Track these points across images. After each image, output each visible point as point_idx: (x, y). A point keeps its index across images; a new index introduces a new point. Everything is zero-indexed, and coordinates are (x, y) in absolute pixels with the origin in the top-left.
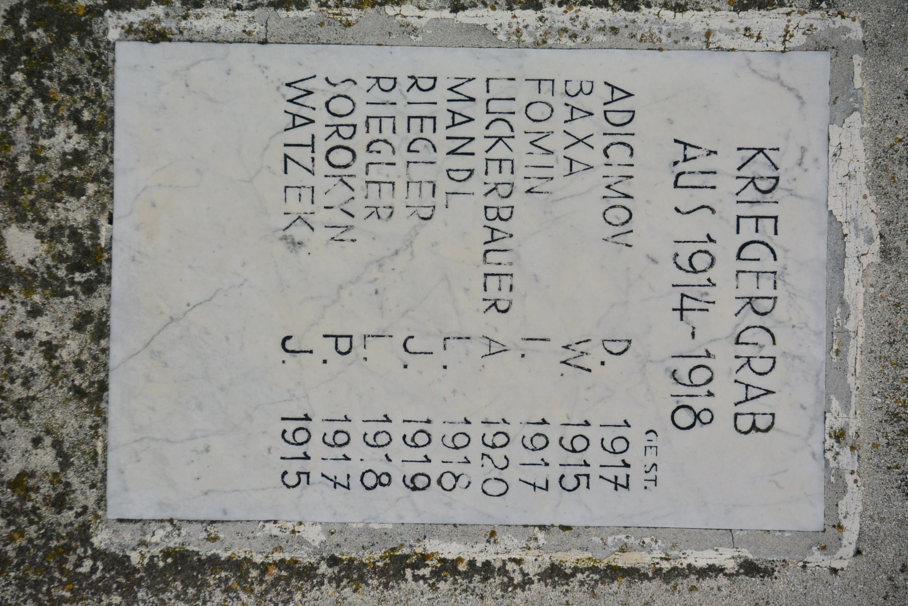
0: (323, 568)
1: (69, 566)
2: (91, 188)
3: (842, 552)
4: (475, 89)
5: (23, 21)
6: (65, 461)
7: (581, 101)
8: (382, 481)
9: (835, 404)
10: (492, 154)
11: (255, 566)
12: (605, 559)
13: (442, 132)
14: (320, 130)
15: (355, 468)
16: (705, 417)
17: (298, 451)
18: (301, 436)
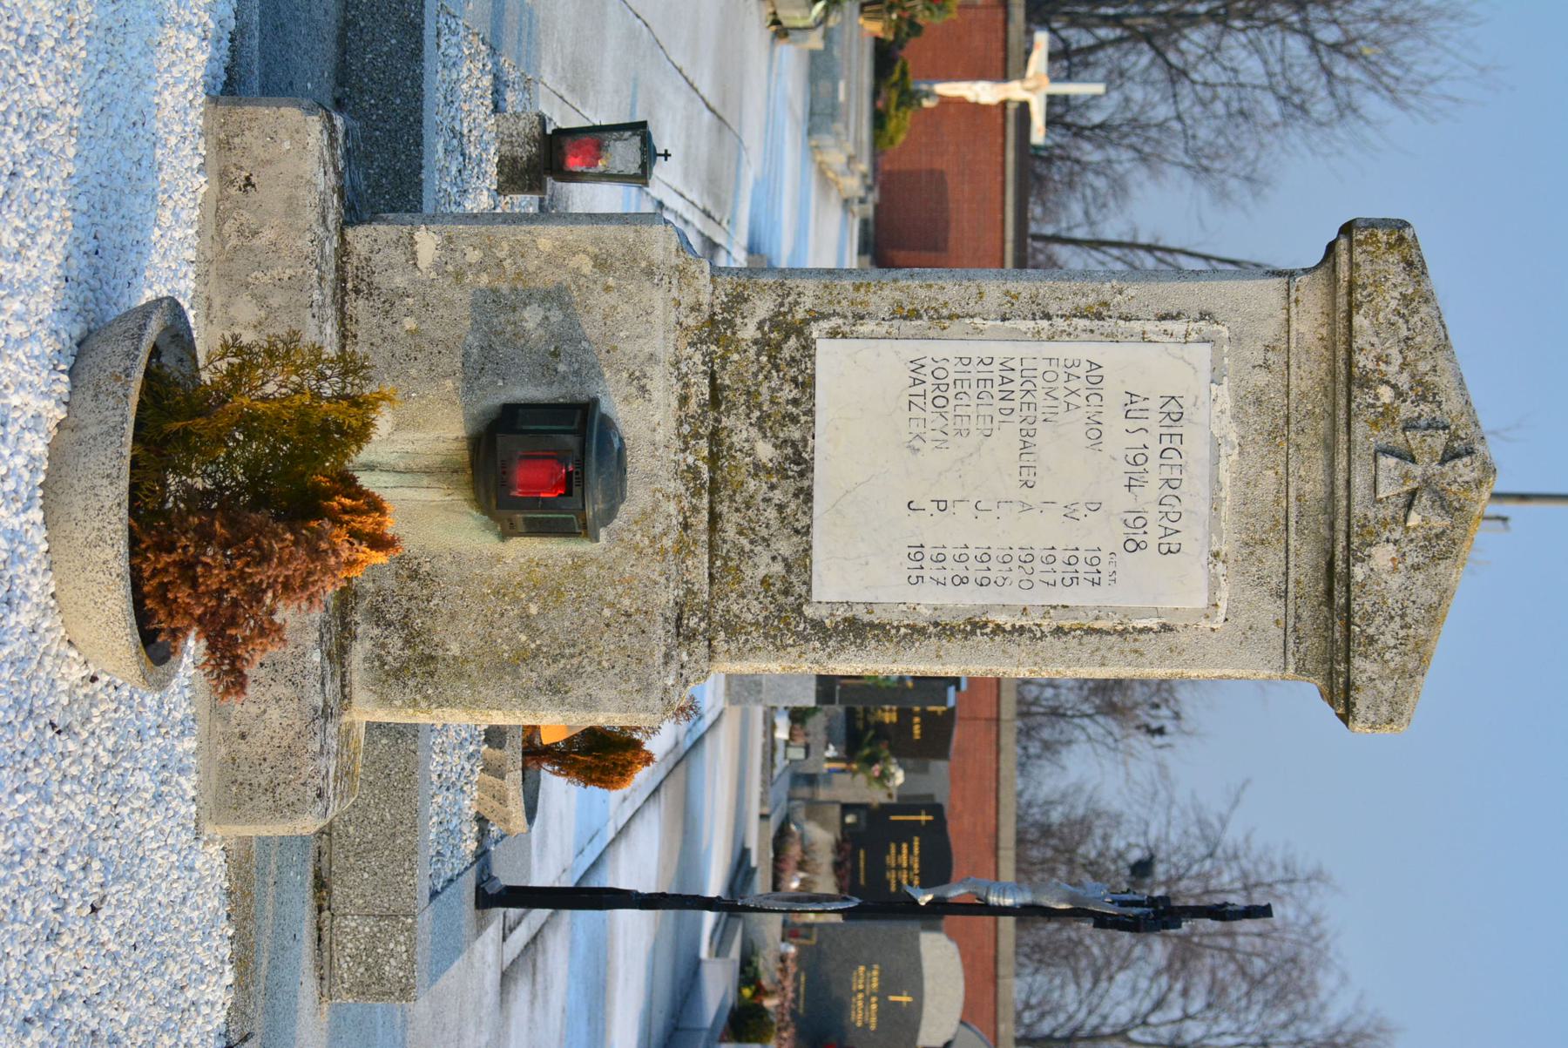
0: (931, 628)
1: (792, 627)
3: (1218, 619)
4: (1015, 364)
5: (766, 329)
6: (789, 568)
8: (964, 581)
9: (1214, 538)
10: (1024, 400)
11: (893, 627)
12: (1088, 623)
13: (997, 388)
14: (929, 387)
16: (1143, 545)
17: (917, 564)
18: (919, 556)
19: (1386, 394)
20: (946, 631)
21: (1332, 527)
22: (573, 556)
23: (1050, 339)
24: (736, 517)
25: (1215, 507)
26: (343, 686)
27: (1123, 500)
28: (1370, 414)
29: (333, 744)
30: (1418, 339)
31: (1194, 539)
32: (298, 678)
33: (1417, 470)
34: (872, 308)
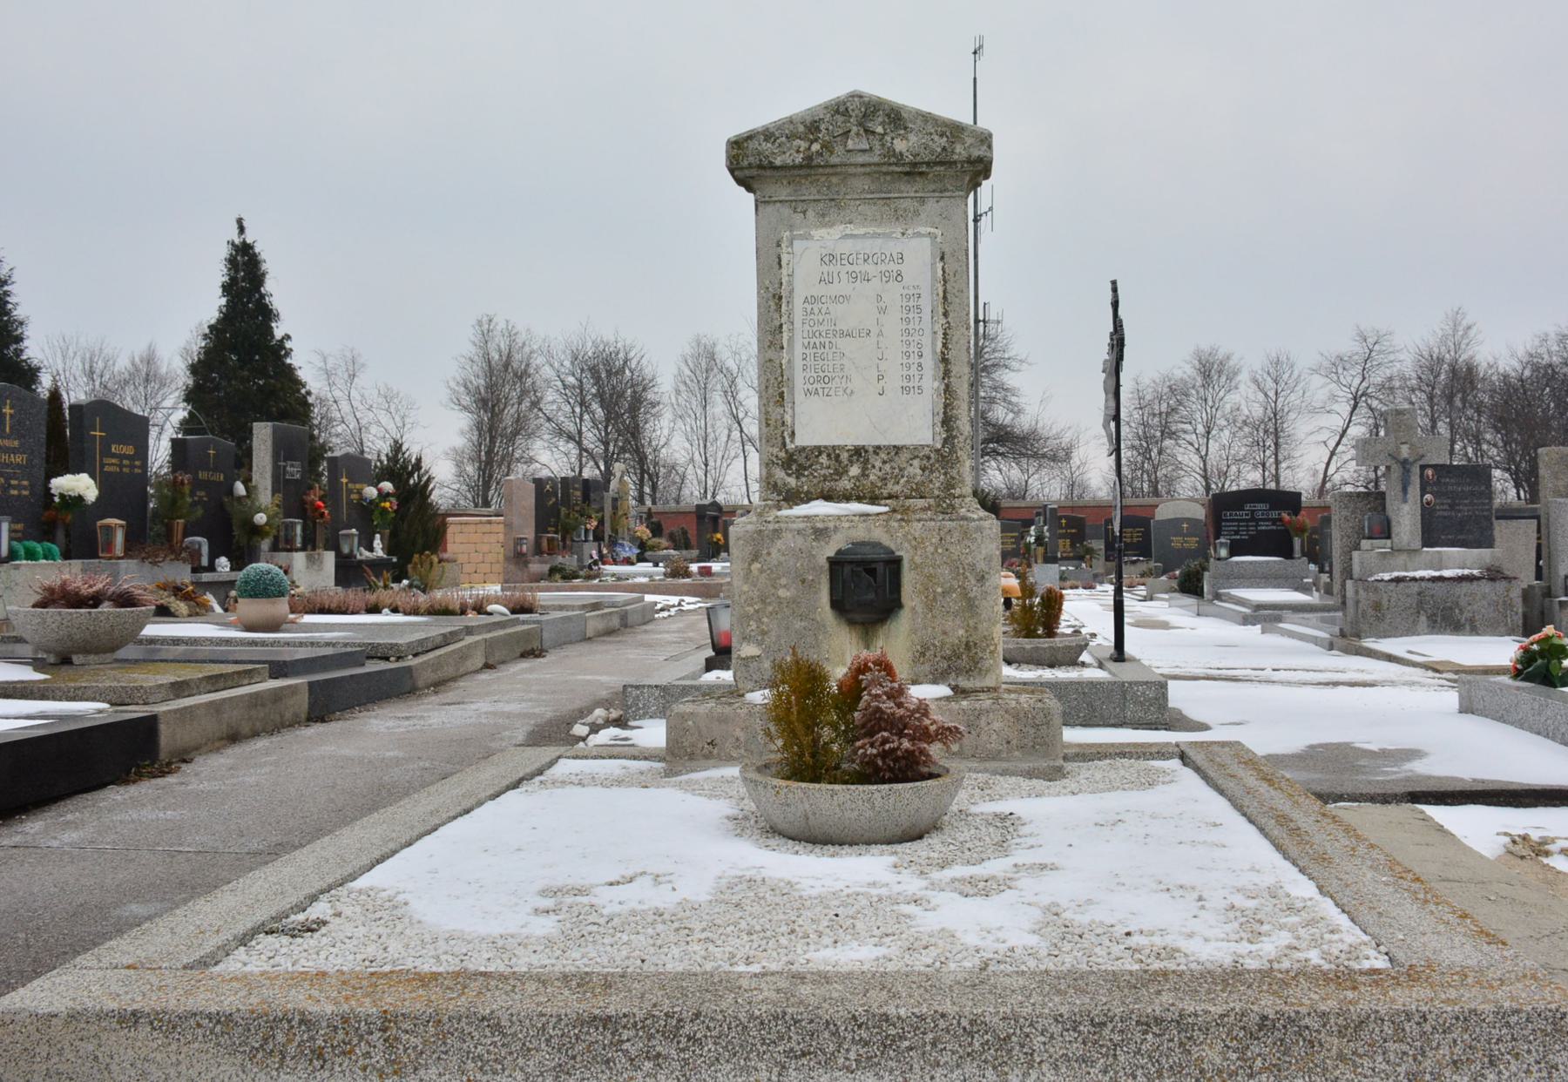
2: (837, 452)
4: (806, 342)
6: (917, 457)
7: (809, 311)
14: (819, 386)
15: (916, 373)
19: (816, 147)
20: (947, 374)
21: (886, 174)
22: (911, 570)
23: (792, 323)
24: (890, 486)
25: (876, 236)
26: (983, 691)
28: (826, 155)
29: (1013, 696)
30: (787, 132)
31: (893, 247)
32: (977, 713)
33: (855, 129)
34: (779, 417)
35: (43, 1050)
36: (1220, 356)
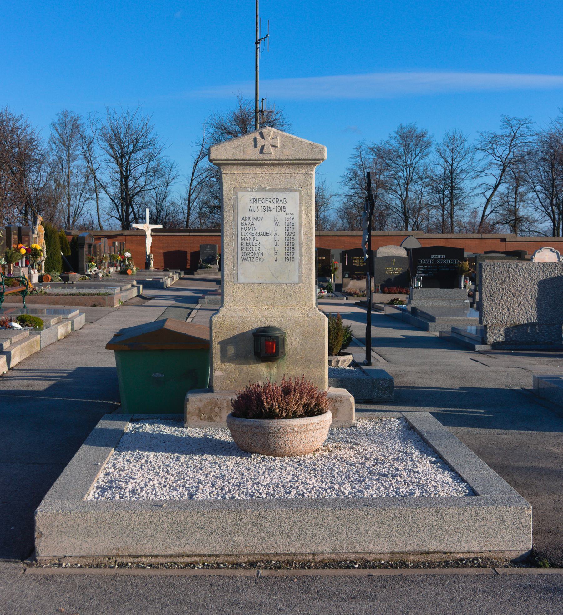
4: (243, 237)
7: (244, 223)
15: (292, 252)
27: (274, 212)
35: (56, 524)
36: (418, 132)
